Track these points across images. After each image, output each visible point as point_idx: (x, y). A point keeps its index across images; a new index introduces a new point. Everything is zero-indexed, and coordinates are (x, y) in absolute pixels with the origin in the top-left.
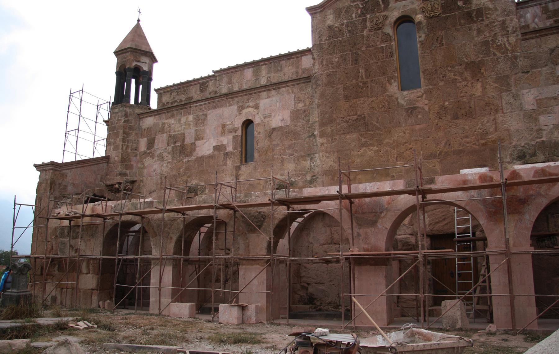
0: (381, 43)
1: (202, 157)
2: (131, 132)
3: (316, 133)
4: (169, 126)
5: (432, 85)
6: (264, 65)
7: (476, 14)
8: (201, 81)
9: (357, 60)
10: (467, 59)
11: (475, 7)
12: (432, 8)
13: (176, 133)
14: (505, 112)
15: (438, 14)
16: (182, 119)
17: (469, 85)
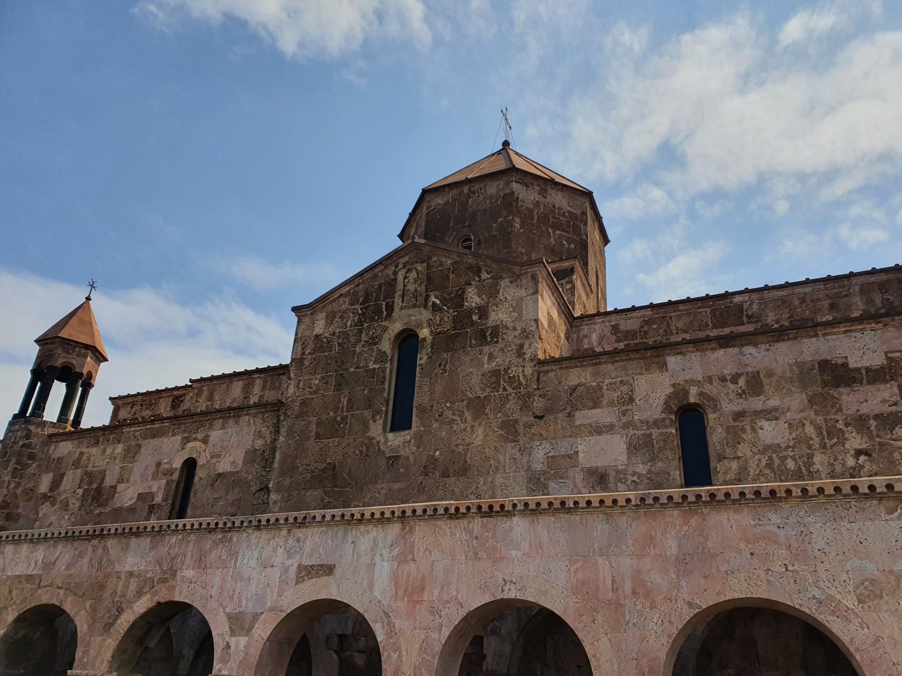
0: (374, 363)
1: (121, 508)
2: (30, 462)
3: (270, 485)
4: (89, 459)
5: (424, 426)
6: (258, 378)
7: (490, 335)
8: (176, 393)
9: (340, 385)
10: (471, 393)
11: (491, 324)
12: (440, 321)
13: (95, 469)
14: (507, 471)
15: (446, 329)
17: (469, 429)
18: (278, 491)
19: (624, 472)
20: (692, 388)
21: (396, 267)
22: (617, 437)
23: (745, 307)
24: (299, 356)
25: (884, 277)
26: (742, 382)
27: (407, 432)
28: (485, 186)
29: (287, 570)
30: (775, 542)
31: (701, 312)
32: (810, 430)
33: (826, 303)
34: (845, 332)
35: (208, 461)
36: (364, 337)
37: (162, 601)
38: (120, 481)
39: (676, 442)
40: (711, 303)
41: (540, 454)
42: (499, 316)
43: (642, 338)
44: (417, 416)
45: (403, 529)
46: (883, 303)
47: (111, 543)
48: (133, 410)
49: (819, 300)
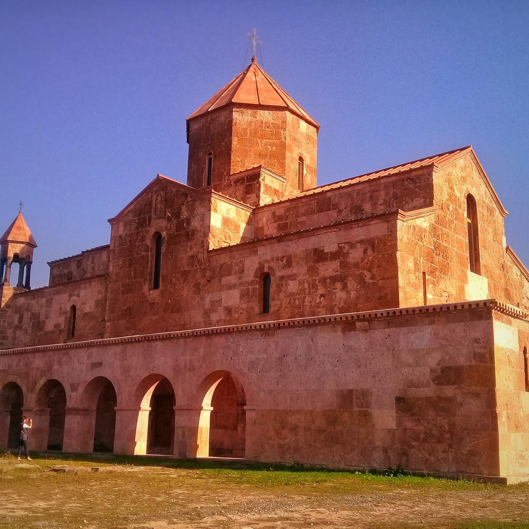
1: (48, 332)
2: (7, 309)
3: (106, 318)
4: (32, 306)
9: (130, 264)
19: (237, 308)
20: (266, 264)
21: (152, 193)
22: (237, 290)
23: (332, 199)
25: (394, 178)
28: (219, 115)
30: (230, 349)
31: (312, 203)
32: (306, 285)
33: (368, 196)
34: (325, 233)
35: (80, 306)
36: (139, 238)
38: (47, 318)
40: (316, 197)
43: (285, 220)
44: (161, 281)
46: (393, 195)
47: (29, 355)
48: (59, 270)
49: (365, 194)
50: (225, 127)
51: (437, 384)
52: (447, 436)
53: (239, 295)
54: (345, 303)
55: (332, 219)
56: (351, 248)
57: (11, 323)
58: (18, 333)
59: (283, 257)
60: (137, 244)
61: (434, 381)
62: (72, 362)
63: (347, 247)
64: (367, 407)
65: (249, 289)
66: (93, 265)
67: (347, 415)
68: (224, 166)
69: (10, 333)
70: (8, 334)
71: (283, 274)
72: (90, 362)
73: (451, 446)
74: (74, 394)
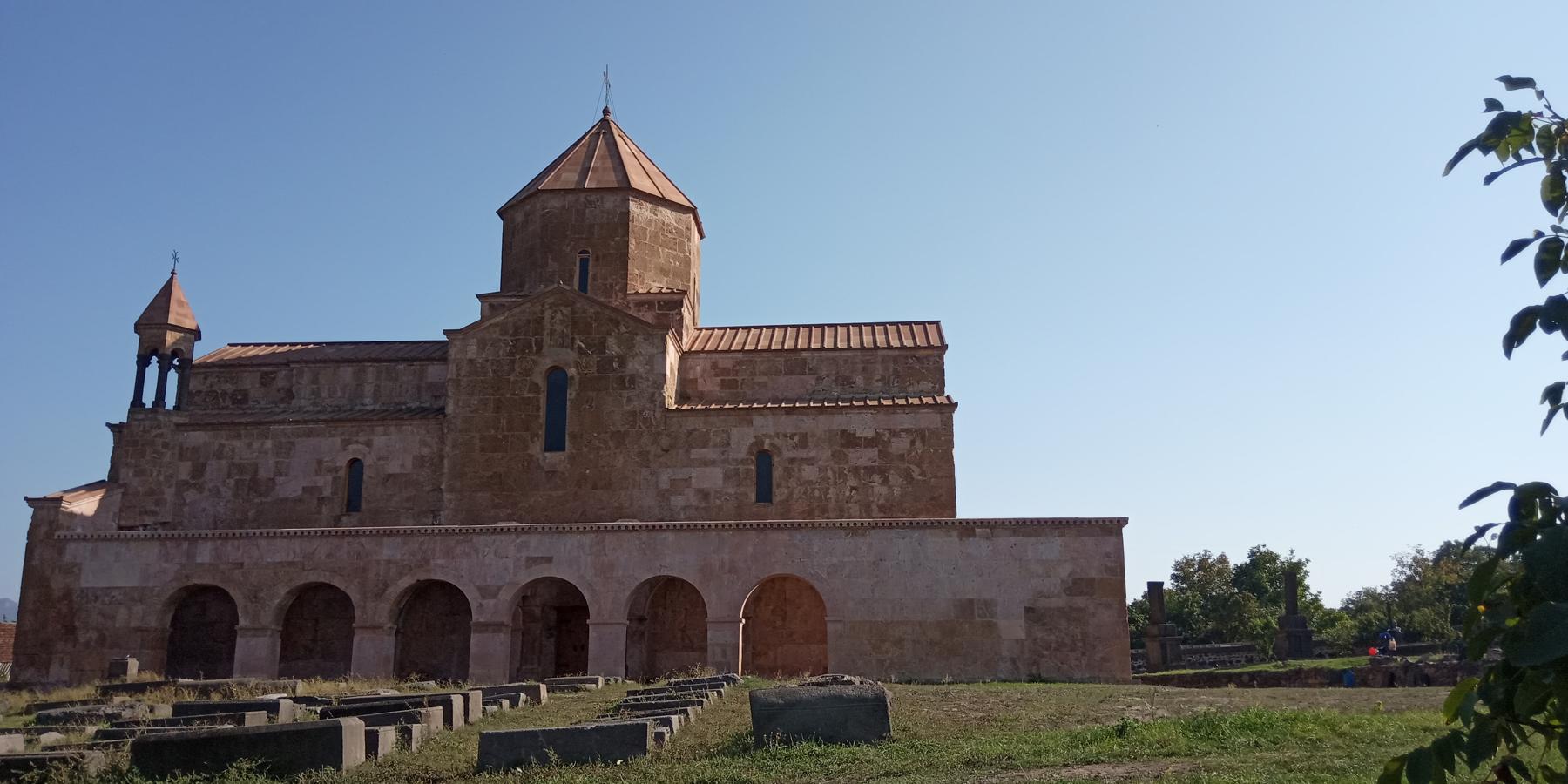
2: (164, 451)
3: (443, 487)
4: (233, 451)
9: (498, 407)
16: (254, 443)
18: (451, 489)
21: (543, 306)
22: (718, 469)
24: (454, 377)
26: (796, 438)
27: (561, 453)
28: (602, 198)
29: (518, 559)
32: (830, 473)
33: (860, 366)
35: (375, 463)
36: (518, 370)
37: (422, 579)
39: (754, 475)
41: (665, 478)
42: (635, 366)
45: (596, 537)
47: (363, 540)
49: (856, 363)
50: (616, 220)
51: (1068, 595)
52: (1080, 644)
53: (721, 476)
54: (887, 500)
55: (808, 387)
56: (894, 436)
57: (172, 477)
58: (190, 495)
59: (794, 434)
60: (512, 378)
61: (1064, 591)
62: (480, 555)
63: (887, 435)
64: (992, 617)
65: (738, 469)
66: (315, 386)
67: (967, 626)
68: (614, 277)
69: (169, 493)
70: (165, 496)
71: (794, 456)
72: (524, 554)
73: (1083, 654)
74: (490, 603)
